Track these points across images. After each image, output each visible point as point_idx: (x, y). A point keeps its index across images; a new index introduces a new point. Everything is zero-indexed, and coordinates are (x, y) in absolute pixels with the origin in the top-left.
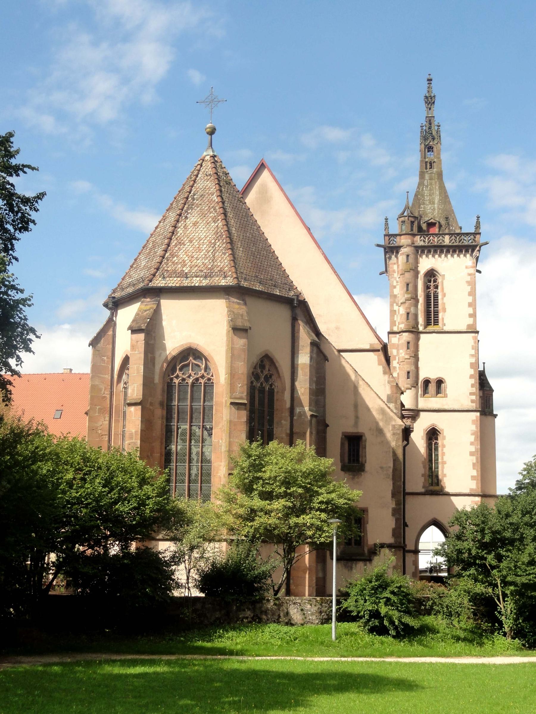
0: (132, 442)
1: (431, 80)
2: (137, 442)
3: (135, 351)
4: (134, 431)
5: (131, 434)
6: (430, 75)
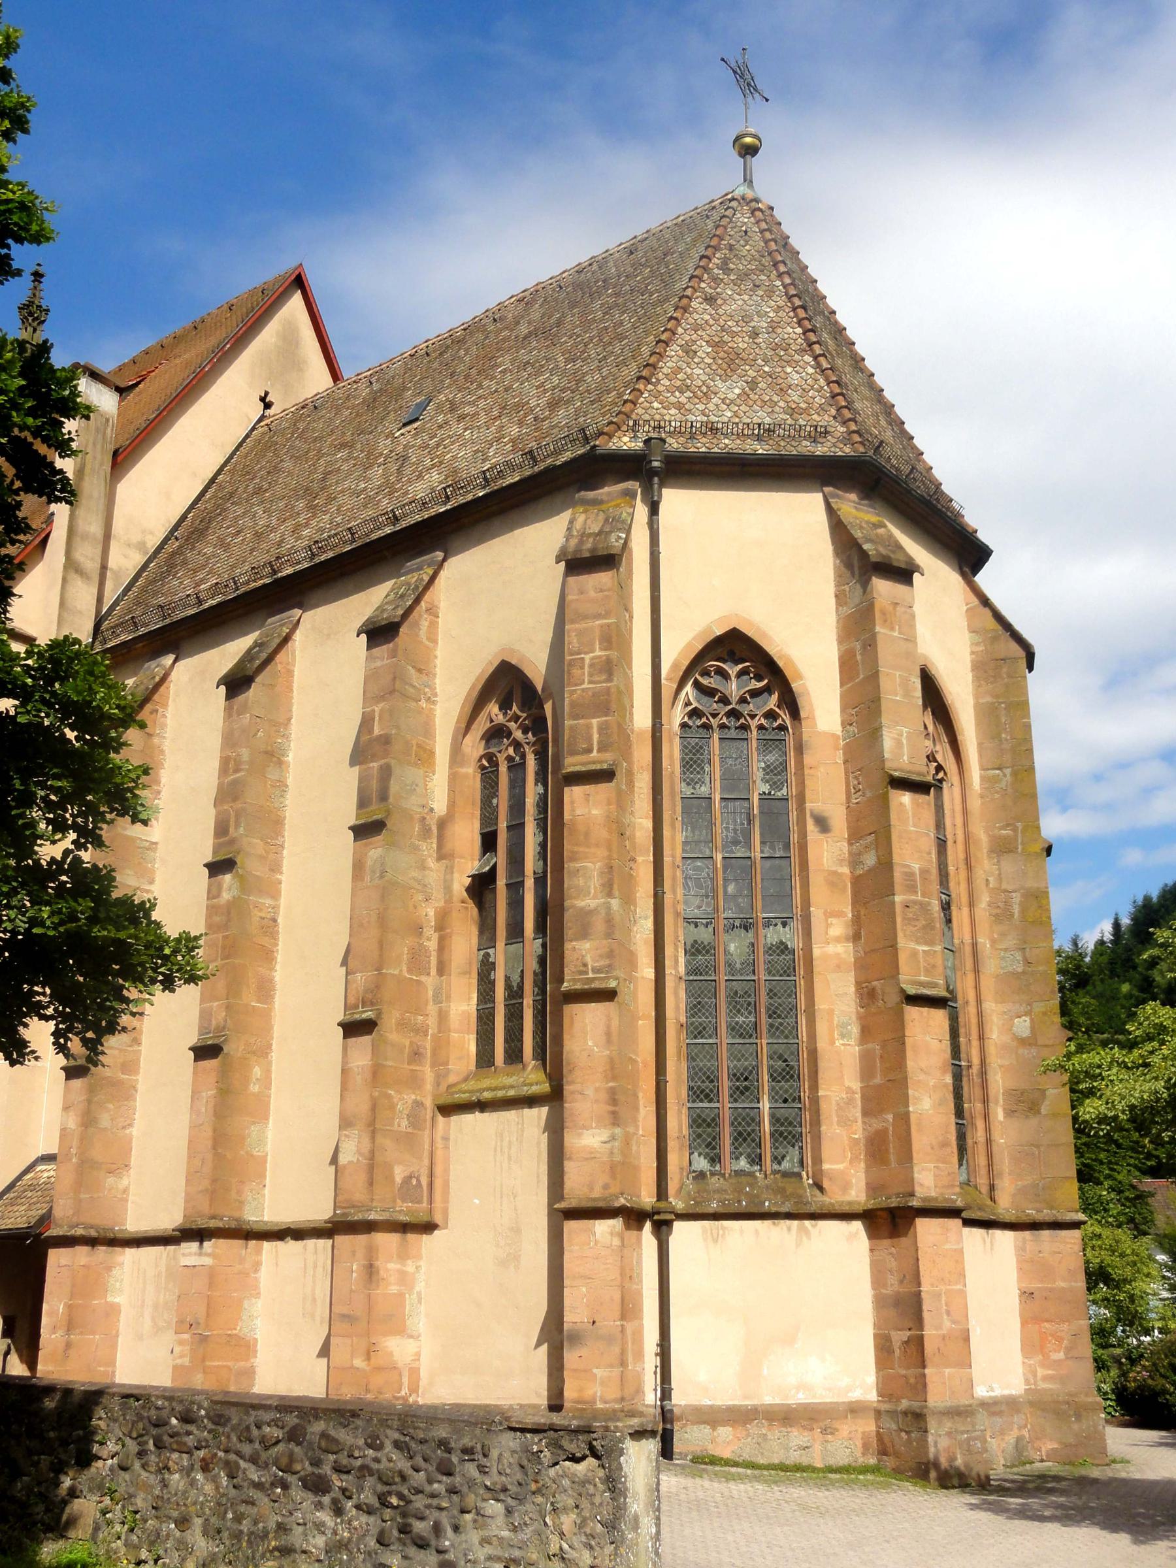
0: (915, 902)
1: (42, 276)
2: (929, 904)
3: (892, 629)
4: (916, 867)
5: (910, 875)
6: (39, 265)
